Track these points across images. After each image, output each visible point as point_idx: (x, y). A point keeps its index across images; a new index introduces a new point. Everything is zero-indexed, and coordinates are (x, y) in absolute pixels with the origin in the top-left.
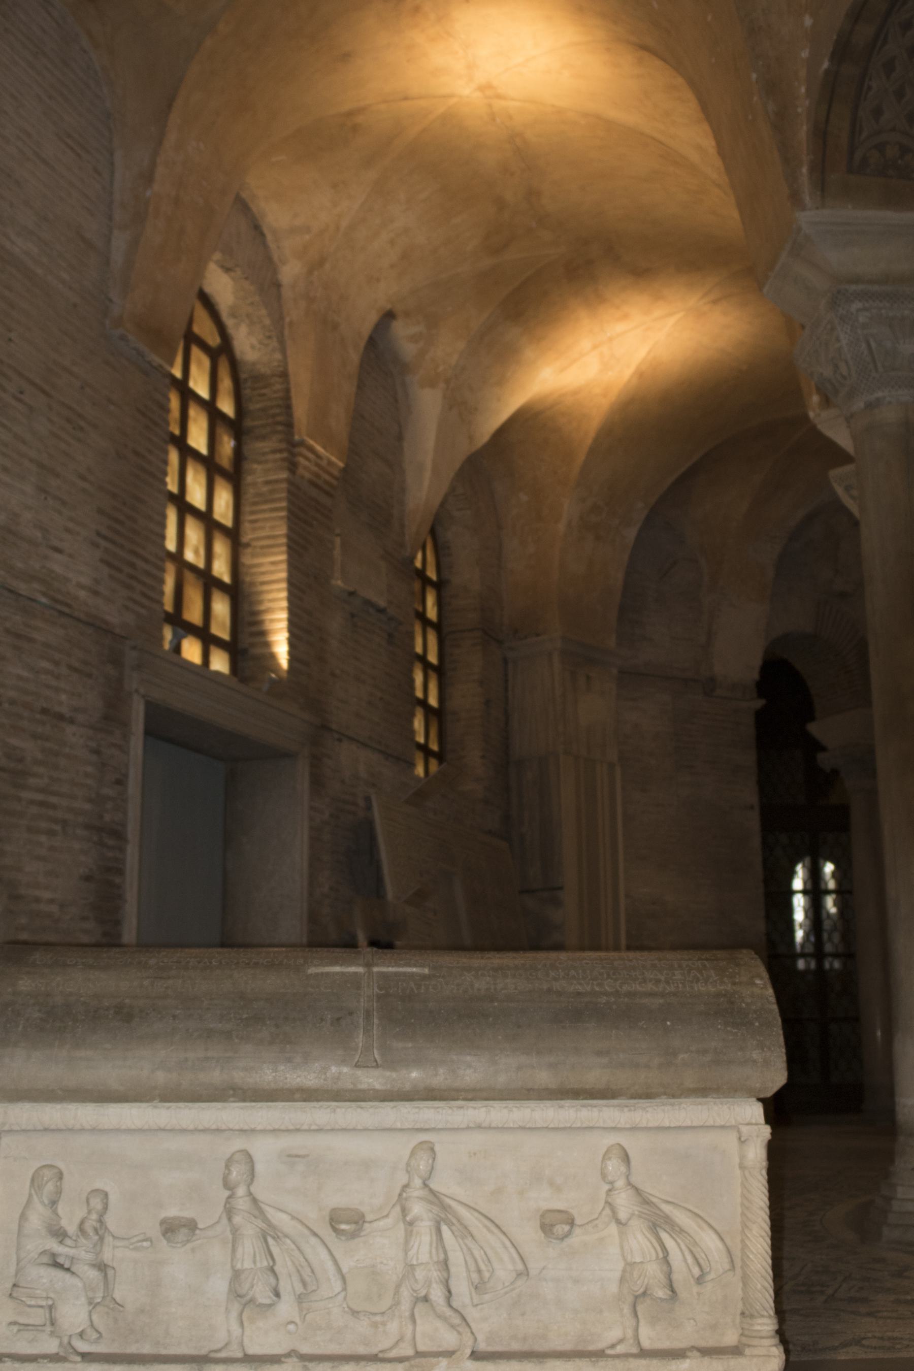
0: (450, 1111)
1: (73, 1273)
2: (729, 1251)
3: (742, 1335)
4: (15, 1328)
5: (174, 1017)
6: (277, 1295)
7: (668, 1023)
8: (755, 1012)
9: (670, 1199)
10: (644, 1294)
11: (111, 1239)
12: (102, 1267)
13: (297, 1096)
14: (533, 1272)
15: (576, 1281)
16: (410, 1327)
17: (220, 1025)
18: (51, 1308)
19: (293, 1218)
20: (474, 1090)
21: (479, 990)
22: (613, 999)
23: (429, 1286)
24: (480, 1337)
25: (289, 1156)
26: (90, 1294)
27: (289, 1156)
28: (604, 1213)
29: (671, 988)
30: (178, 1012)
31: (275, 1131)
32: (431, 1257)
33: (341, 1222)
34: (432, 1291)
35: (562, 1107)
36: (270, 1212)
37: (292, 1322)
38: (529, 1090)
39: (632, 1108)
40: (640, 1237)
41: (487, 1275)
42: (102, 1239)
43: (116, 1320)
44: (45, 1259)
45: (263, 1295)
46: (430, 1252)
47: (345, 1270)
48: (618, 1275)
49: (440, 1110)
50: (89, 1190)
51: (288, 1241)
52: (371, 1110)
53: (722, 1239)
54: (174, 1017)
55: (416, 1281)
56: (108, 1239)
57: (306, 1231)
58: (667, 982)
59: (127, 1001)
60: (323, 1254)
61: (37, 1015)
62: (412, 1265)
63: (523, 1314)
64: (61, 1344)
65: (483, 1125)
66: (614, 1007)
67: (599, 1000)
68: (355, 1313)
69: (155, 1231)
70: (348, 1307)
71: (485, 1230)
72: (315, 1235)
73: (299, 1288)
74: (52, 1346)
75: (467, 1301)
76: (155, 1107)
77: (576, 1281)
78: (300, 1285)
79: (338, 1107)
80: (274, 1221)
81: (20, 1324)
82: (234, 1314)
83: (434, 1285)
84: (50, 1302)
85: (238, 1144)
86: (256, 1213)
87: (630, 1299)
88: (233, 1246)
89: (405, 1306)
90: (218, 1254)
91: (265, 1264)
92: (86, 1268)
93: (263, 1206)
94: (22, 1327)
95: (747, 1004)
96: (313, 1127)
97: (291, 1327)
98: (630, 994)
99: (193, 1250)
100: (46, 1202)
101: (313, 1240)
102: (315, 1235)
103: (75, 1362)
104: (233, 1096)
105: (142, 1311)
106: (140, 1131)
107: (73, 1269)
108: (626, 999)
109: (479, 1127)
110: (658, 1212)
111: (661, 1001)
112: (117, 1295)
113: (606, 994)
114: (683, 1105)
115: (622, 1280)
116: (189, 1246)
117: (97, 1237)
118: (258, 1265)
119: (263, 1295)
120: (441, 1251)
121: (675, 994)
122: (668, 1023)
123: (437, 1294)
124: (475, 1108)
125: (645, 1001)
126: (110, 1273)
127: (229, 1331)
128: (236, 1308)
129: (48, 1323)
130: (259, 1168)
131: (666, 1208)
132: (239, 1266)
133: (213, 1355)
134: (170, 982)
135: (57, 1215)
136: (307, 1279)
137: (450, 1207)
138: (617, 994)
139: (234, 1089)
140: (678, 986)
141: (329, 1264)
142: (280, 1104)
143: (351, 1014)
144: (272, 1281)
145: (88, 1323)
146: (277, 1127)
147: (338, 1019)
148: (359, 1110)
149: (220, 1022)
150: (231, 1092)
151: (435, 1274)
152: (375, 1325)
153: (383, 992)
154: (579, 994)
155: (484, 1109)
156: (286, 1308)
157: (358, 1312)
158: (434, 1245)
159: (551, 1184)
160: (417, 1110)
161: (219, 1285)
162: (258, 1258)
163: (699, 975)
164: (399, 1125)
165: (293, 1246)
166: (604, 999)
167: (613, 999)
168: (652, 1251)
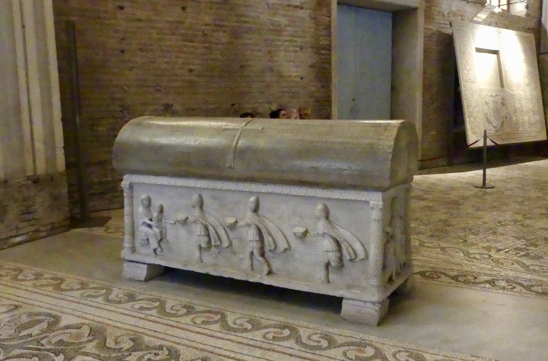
18: (148, 240)
32: (253, 239)
34: (254, 250)
39: (328, 190)
40: (327, 241)
56: (163, 220)
60: (223, 232)
83: (254, 249)
84: (146, 238)
109: (271, 193)
126: (164, 231)
135: (150, 211)
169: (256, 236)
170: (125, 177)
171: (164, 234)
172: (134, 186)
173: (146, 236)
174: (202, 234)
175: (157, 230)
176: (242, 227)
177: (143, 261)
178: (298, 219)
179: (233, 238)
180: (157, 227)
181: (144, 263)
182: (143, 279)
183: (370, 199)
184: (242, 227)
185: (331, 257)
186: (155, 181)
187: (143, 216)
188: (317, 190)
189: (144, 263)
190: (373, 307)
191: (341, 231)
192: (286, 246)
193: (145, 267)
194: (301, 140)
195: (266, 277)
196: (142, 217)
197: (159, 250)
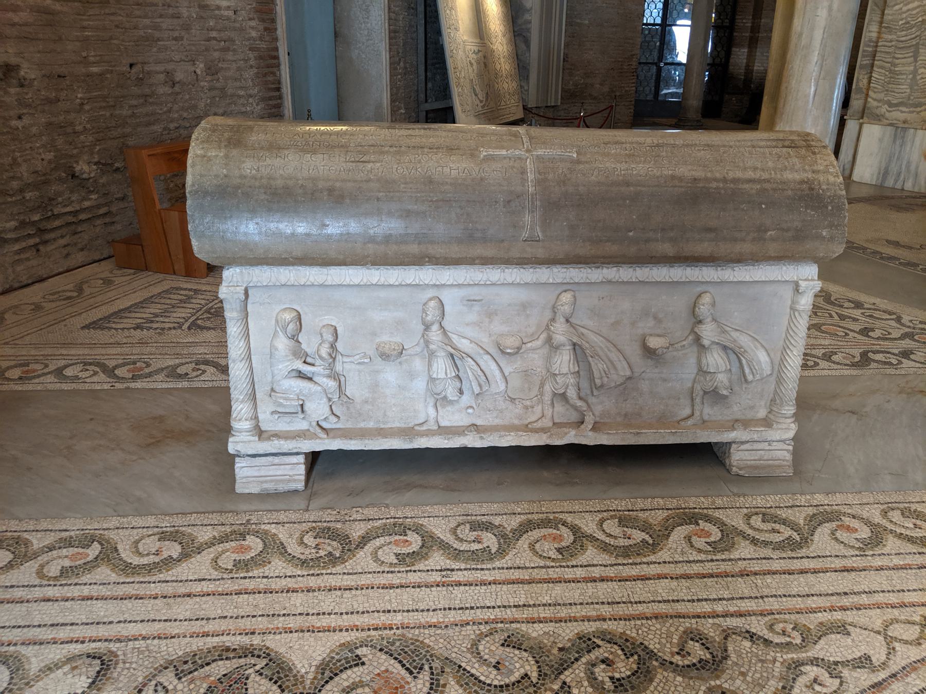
0: (590, 271)
1: (316, 383)
2: (772, 362)
3: (769, 412)
4: (276, 416)
5: (378, 199)
6: (461, 392)
7: (763, 206)
8: (829, 197)
9: (737, 328)
10: (713, 390)
11: (340, 356)
12: (335, 376)
13: (477, 261)
14: (636, 375)
15: (665, 380)
16: (551, 410)
17: (416, 207)
18: (302, 405)
19: (471, 342)
20: (610, 257)
21: (618, 175)
22: (722, 185)
23: (567, 388)
24: (597, 413)
25: (468, 300)
26: (330, 396)
27: (468, 300)
28: (690, 337)
29: (765, 176)
30: (381, 194)
31: (459, 286)
32: (569, 370)
33: (507, 348)
34: (568, 390)
35: (672, 267)
36: (455, 338)
37: (471, 407)
38: (652, 257)
40: (716, 356)
41: (605, 379)
42: (334, 359)
43: (348, 408)
44: (294, 374)
45: (451, 394)
46: (569, 367)
47: (507, 374)
48: (693, 376)
49: (582, 269)
50: (321, 325)
51: (470, 360)
52: (531, 270)
53: (769, 354)
54: (378, 199)
55: (557, 383)
56: (339, 357)
57: (482, 352)
58: (763, 170)
59: (338, 184)
60: (493, 366)
61: (263, 197)
62: (555, 374)
63: (626, 400)
64: (310, 425)
65: (614, 280)
66: (723, 192)
67: (711, 185)
68: (512, 400)
69: (371, 352)
70: (508, 396)
71: (606, 350)
72: (488, 353)
73: (477, 390)
74: (304, 425)
75: (589, 392)
76: (368, 269)
77: (665, 380)
78: (478, 388)
79: (506, 268)
80: (459, 346)
81: (279, 412)
82: (432, 404)
83: (570, 387)
85: (430, 293)
86: (447, 342)
87: (701, 393)
88: (429, 361)
89: (547, 397)
90: (418, 364)
91: (454, 374)
92: (325, 379)
93: (449, 334)
94: (281, 415)
95: (823, 190)
96: (488, 283)
97: (470, 411)
98: (735, 181)
99: (400, 363)
100: (290, 336)
101: (487, 357)
102: (488, 353)
103: (323, 439)
104: (429, 262)
105: (367, 402)
106: (358, 285)
107: (314, 379)
108: (732, 185)
109: (610, 282)
110: (729, 338)
111: (758, 187)
112: (348, 393)
113: (715, 180)
114: (761, 266)
115: (694, 381)
116: (399, 360)
117: (331, 360)
118: (449, 376)
119: (451, 394)
120: (576, 365)
121: (768, 181)
122: (763, 206)
123: (572, 393)
124: (608, 268)
125: (746, 186)
126: (342, 379)
127: (427, 414)
128: (431, 402)
129: (300, 412)
130: (447, 308)
131: (735, 335)
132: (435, 376)
133: (417, 428)
134: (369, 166)
135: (299, 342)
136: (483, 383)
137: (583, 335)
138: (725, 180)
139: (429, 258)
140: (771, 174)
141: (497, 373)
142: (463, 267)
143: (518, 197)
144: (458, 385)
145: (330, 413)
146: (461, 283)
147: (509, 202)
148: (522, 270)
149: (416, 204)
150: (427, 259)
151: (571, 380)
152: (526, 408)
153: (543, 177)
154: (695, 179)
155: (615, 269)
156: (466, 399)
157: (515, 399)
158: (572, 362)
159: (655, 318)
160: (565, 270)
161: (420, 384)
162: (448, 371)
163: (786, 164)
164: (551, 281)
165: (473, 363)
166: (714, 185)
167: (722, 185)
168: (724, 365)
169: (574, 364)
170: (227, 274)
171: (343, 388)
172: (250, 292)
173: (298, 399)
174: (449, 376)
175: (332, 384)
176: (534, 349)
177: (295, 451)
178: (651, 323)
179: (510, 373)
180: (329, 376)
181: (297, 454)
182: (300, 486)
183: (798, 276)
184: (534, 349)
185: (722, 382)
186: (325, 278)
187: (291, 357)
188: (704, 268)
189: (297, 454)
190: (786, 447)
191: (735, 335)
192: (628, 373)
193: (301, 459)
194: (673, 177)
195: (590, 433)
196: (290, 360)
197: (333, 419)
